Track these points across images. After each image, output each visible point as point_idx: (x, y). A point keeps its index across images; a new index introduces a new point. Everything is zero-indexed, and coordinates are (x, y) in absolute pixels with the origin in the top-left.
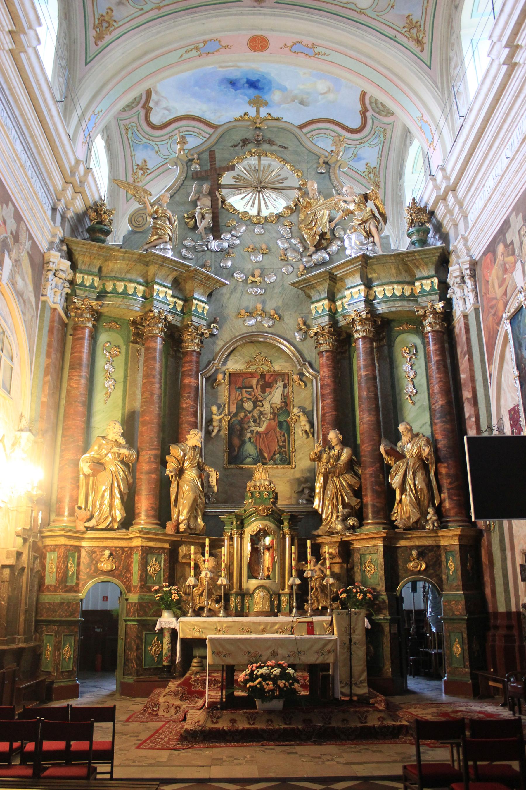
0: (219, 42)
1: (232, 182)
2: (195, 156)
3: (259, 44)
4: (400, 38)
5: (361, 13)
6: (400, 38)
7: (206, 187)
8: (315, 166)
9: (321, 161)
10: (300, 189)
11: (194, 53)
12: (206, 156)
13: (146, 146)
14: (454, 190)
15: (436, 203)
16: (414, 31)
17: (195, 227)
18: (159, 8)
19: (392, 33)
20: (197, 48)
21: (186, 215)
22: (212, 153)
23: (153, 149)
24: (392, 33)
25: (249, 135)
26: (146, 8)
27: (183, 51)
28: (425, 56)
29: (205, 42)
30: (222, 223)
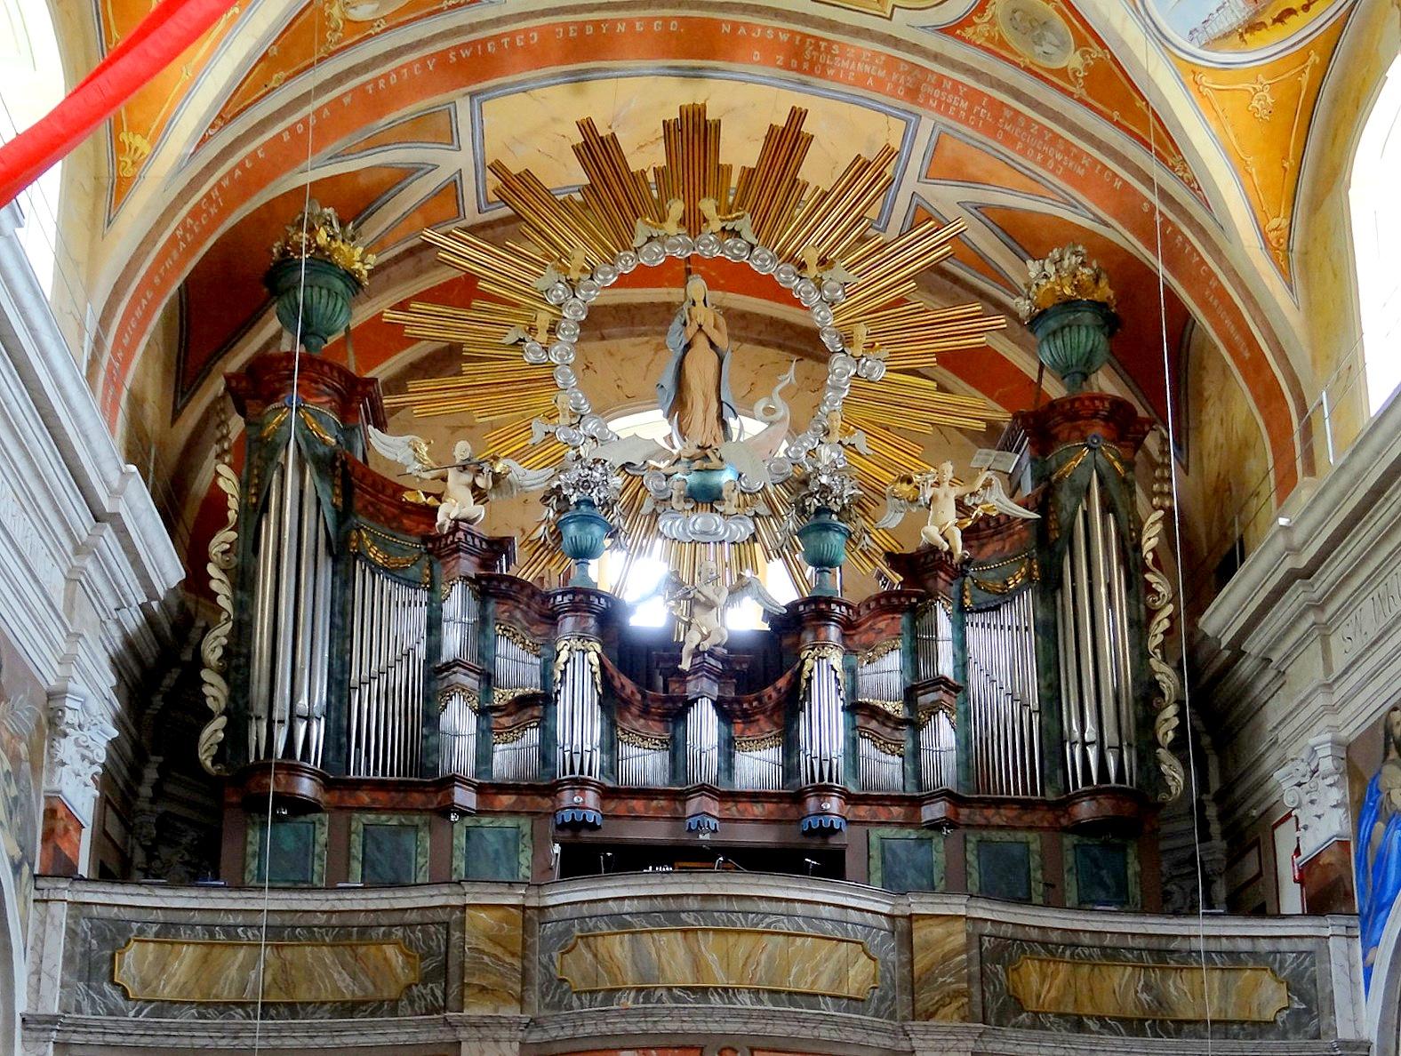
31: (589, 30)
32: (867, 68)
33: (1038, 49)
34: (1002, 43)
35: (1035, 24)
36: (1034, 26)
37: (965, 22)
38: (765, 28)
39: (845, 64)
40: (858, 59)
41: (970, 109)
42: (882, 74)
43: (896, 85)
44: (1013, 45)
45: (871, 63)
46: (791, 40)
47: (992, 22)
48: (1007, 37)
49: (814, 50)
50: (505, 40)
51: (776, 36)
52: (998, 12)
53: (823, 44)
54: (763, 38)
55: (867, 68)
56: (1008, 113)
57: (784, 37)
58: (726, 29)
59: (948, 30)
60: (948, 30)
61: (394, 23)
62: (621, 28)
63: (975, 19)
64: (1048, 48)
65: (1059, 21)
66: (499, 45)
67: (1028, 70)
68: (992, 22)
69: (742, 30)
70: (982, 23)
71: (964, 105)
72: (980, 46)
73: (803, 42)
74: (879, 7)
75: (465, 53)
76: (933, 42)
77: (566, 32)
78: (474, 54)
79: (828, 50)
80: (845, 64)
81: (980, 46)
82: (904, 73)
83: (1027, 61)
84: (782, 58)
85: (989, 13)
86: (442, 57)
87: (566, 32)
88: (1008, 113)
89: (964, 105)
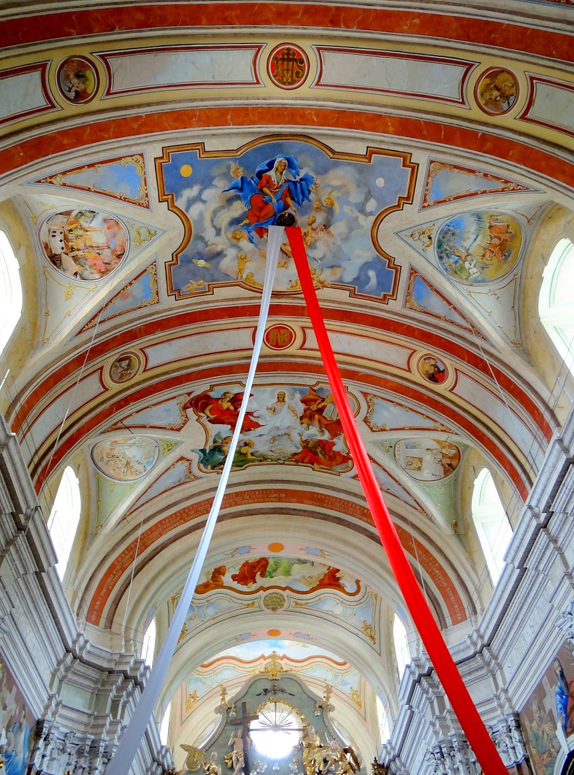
0: (250, 634)
1: (259, 726)
2: (233, 706)
3: (274, 633)
4: (361, 634)
5: (336, 617)
6: (361, 634)
7: (240, 732)
8: (313, 709)
9: (317, 705)
10: (303, 730)
11: (234, 640)
12: (239, 704)
13: (197, 680)
14: (399, 756)
15: (390, 761)
16: (369, 630)
17: (232, 768)
18: (213, 619)
19: (357, 631)
20: (236, 638)
21: (226, 757)
22: (244, 704)
23: (201, 681)
24: (357, 631)
25: (268, 686)
26: (206, 620)
27: (227, 641)
28: (376, 647)
29: (241, 635)
30: (250, 763)
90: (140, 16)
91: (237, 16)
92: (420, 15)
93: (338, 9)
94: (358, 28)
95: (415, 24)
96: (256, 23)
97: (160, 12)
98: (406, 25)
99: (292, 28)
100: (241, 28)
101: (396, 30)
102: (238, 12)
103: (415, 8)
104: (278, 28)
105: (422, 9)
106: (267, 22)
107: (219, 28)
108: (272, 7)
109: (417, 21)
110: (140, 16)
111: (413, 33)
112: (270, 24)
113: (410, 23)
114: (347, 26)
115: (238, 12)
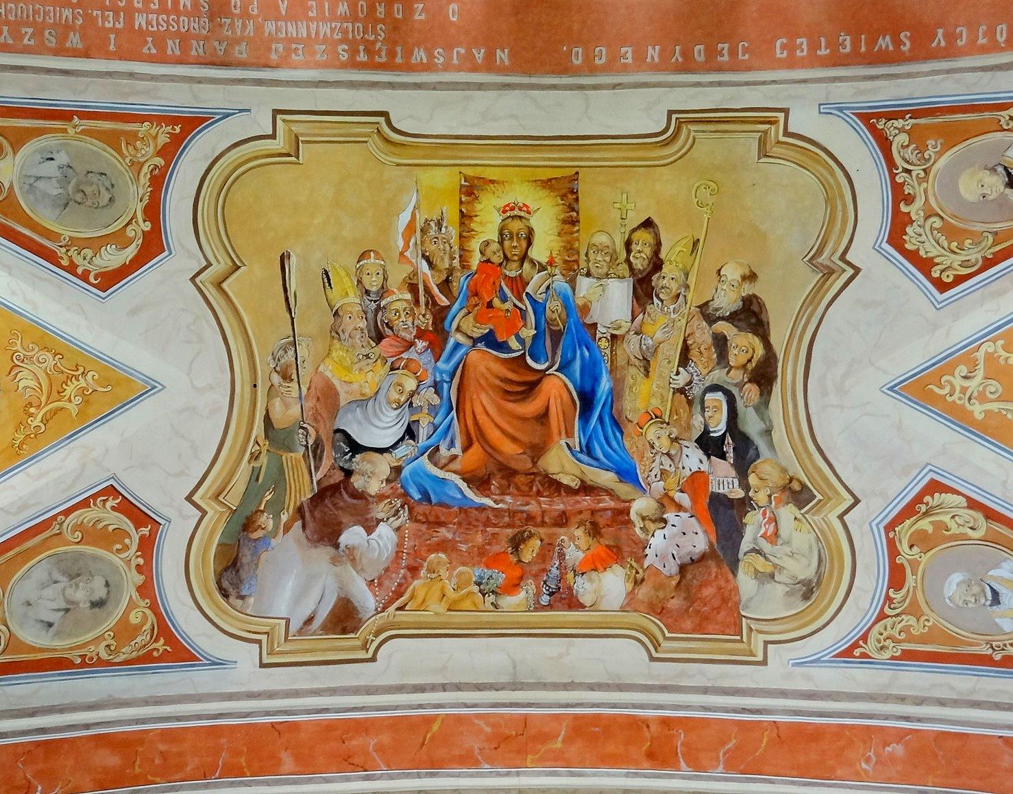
31: (699, 52)
32: (292, 30)
33: (62, 158)
34: (112, 139)
35: (79, 197)
36: (80, 192)
37: (171, 151)
38: (447, 67)
39: (325, 29)
40: (309, 42)
41: (130, 19)
42: (270, 27)
43: (245, 15)
44: (94, 145)
45: (289, 40)
46: (408, 53)
47: (136, 166)
48: (108, 154)
49: (374, 43)
50: (823, 52)
51: (431, 56)
52: (133, 188)
53: (362, 57)
54: (449, 47)
55: (292, 30)
56: (74, 41)
57: (420, 55)
58: (503, 56)
59: (189, 125)
60: (189, 125)
61: (987, 115)
62: (653, 53)
63: (160, 161)
64: (50, 169)
65: (47, 217)
66: (833, 44)
67: (66, 116)
68: (136, 166)
69: (480, 55)
70: (149, 156)
71: (140, 20)
72: (141, 119)
73: (392, 54)
74: (295, 128)
75: (885, 42)
76: (210, 98)
77: (733, 52)
78: (872, 42)
79: (354, 52)
80: (325, 29)
81: (141, 119)
82: (237, 41)
83: (71, 131)
84: (417, 17)
85: (144, 179)
86: (923, 52)
87: (733, 52)
88: (74, 41)
89: (140, 20)
90: (111, 760)
91: (380, 749)
92: (901, 735)
93: (666, 722)
94: (729, 767)
95: (892, 759)
96: (434, 764)
97: (162, 747)
98: (868, 760)
99: (539, 774)
100: (391, 778)
101: (839, 772)
102: (385, 738)
103: (886, 718)
104: (499, 775)
105: (907, 719)
106: (467, 760)
107: (327, 781)
108: (481, 723)
109: (897, 749)
110: (111, 760)
111: (889, 780)
112: (476, 764)
113: (877, 755)
114: (697, 765)
115: (385, 738)
